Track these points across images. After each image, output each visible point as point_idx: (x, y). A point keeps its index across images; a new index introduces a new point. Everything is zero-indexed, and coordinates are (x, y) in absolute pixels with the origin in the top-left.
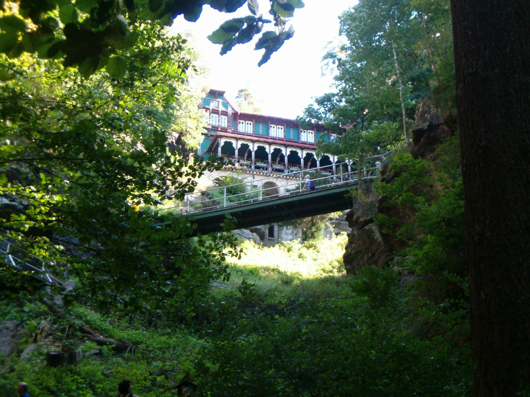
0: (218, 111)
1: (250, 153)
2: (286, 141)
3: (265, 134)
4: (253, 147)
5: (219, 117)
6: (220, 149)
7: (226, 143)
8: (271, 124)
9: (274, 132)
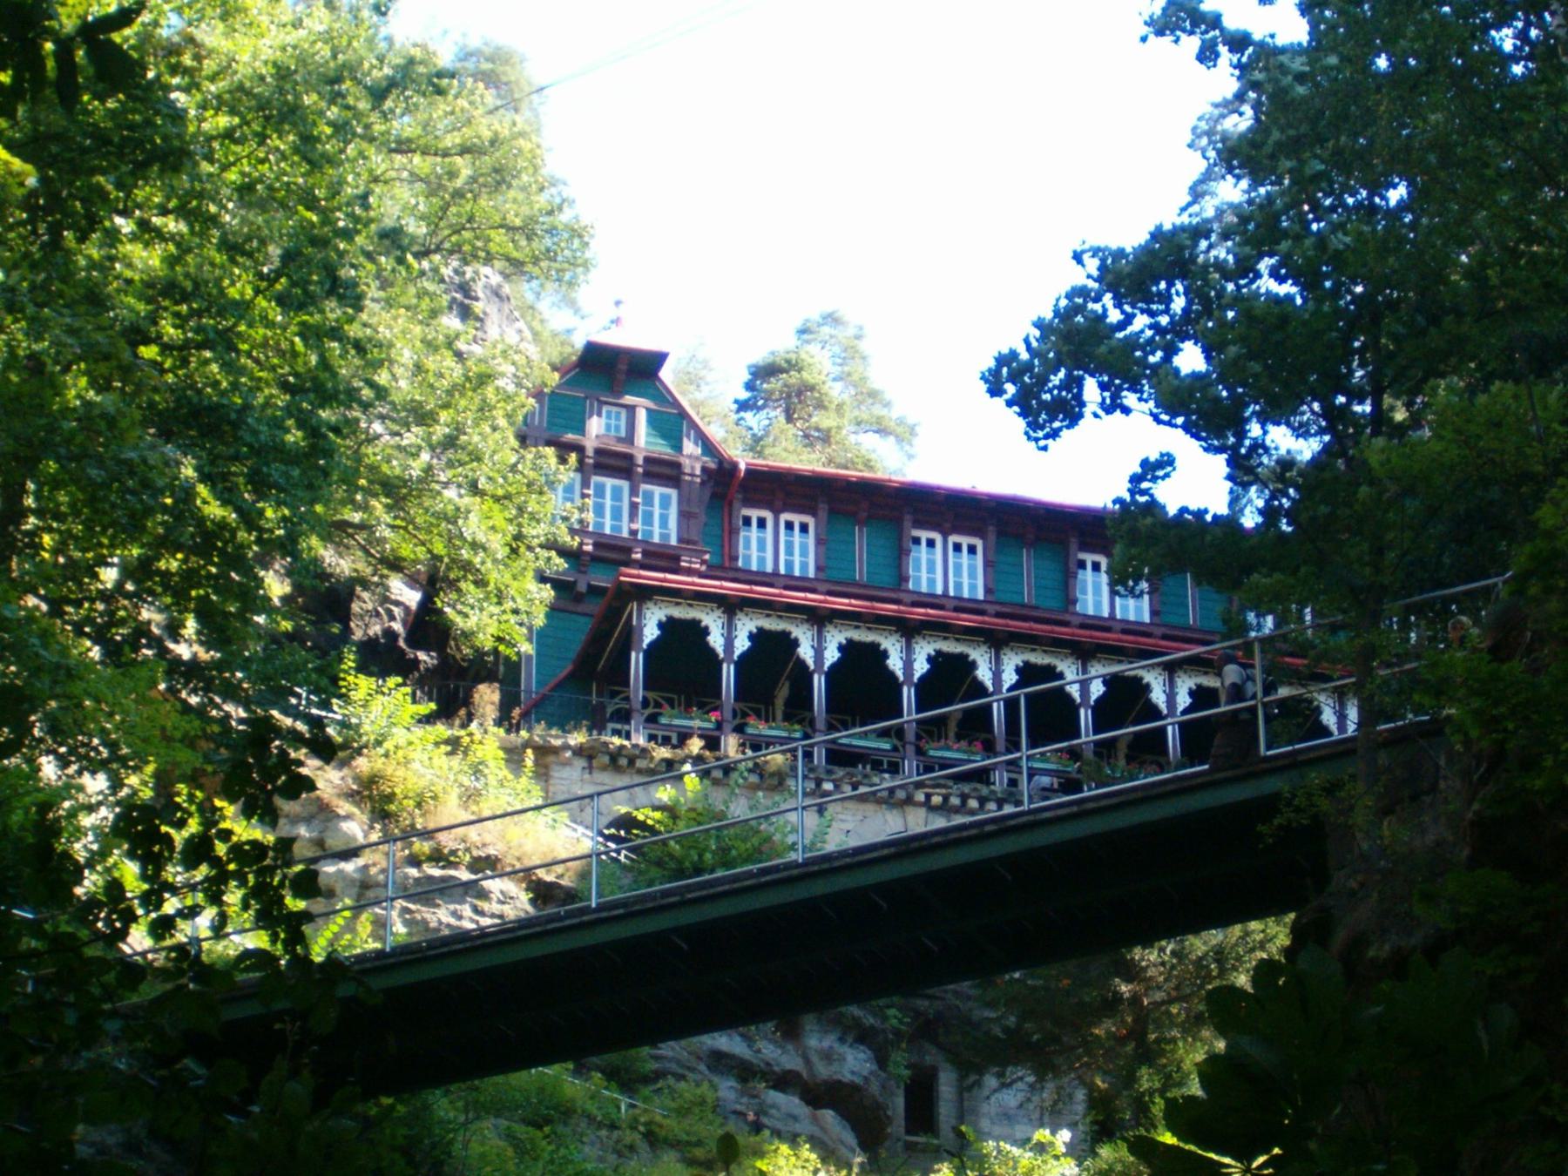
0: (629, 458)
1: (802, 675)
2: (998, 615)
3: (886, 578)
4: (817, 650)
5: (634, 491)
6: (636, 661)
7: (669, 627)
8: (1085, 547)
9: (931, 569)
